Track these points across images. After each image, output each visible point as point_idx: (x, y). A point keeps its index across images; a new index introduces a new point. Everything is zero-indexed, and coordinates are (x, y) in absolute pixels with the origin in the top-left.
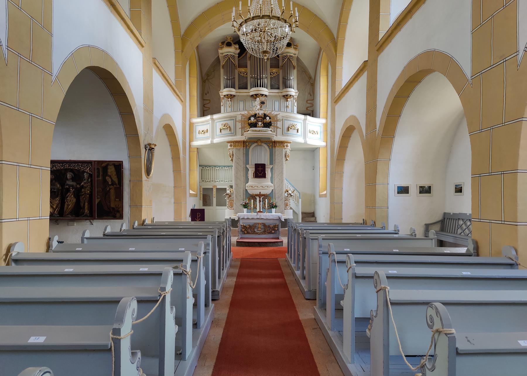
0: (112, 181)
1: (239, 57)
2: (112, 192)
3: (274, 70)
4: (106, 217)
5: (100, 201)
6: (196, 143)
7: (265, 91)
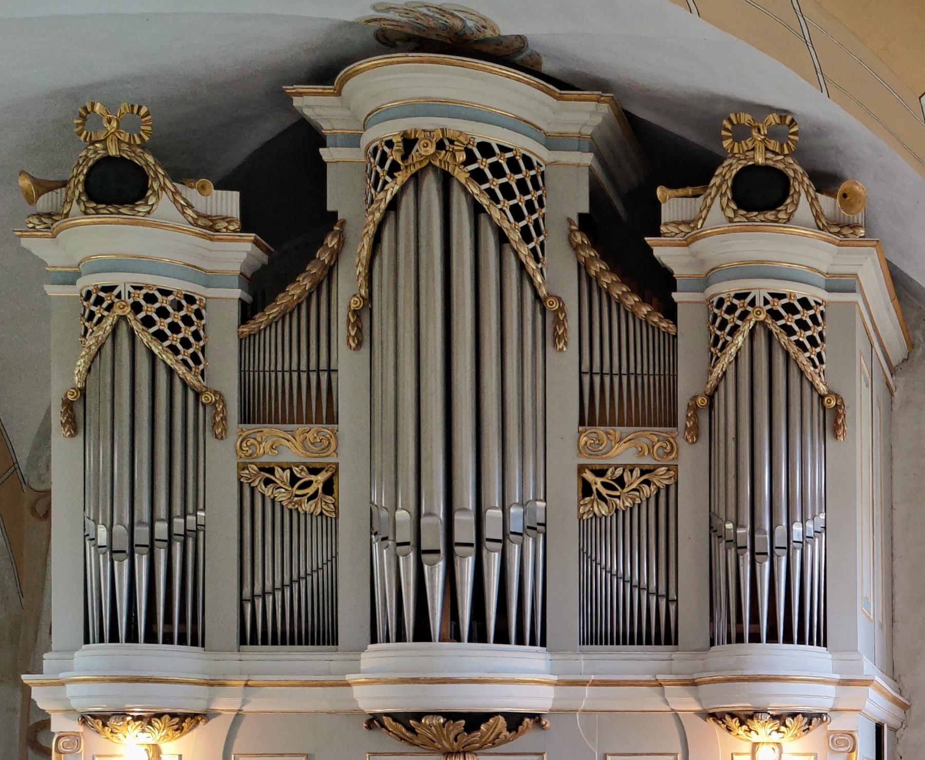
3: (624, 449)
7: (513, 678)
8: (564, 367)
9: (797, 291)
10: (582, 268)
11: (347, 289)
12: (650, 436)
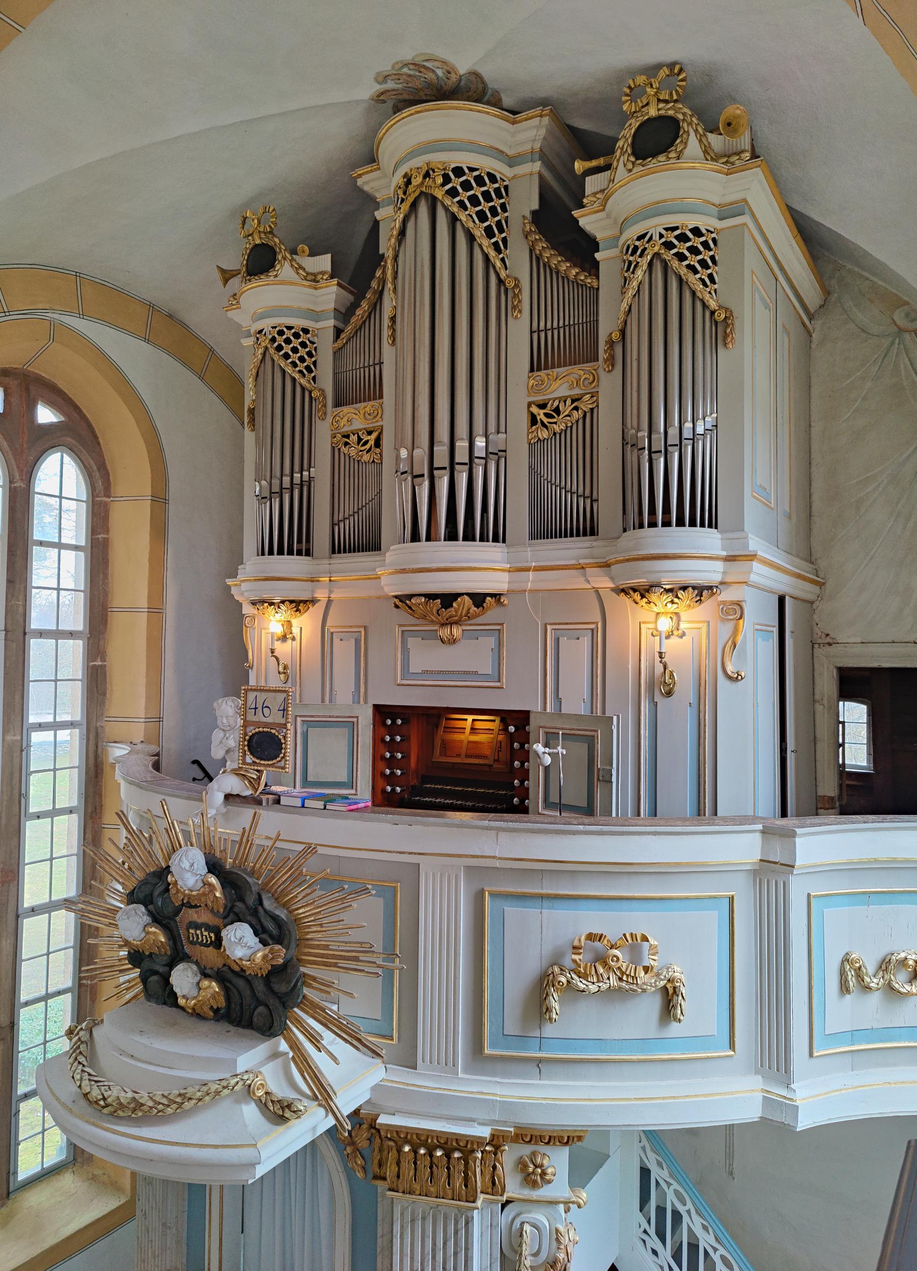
1: (338, 332)
3: (560, 385)
7: (480, 567)
12: (578, 371)
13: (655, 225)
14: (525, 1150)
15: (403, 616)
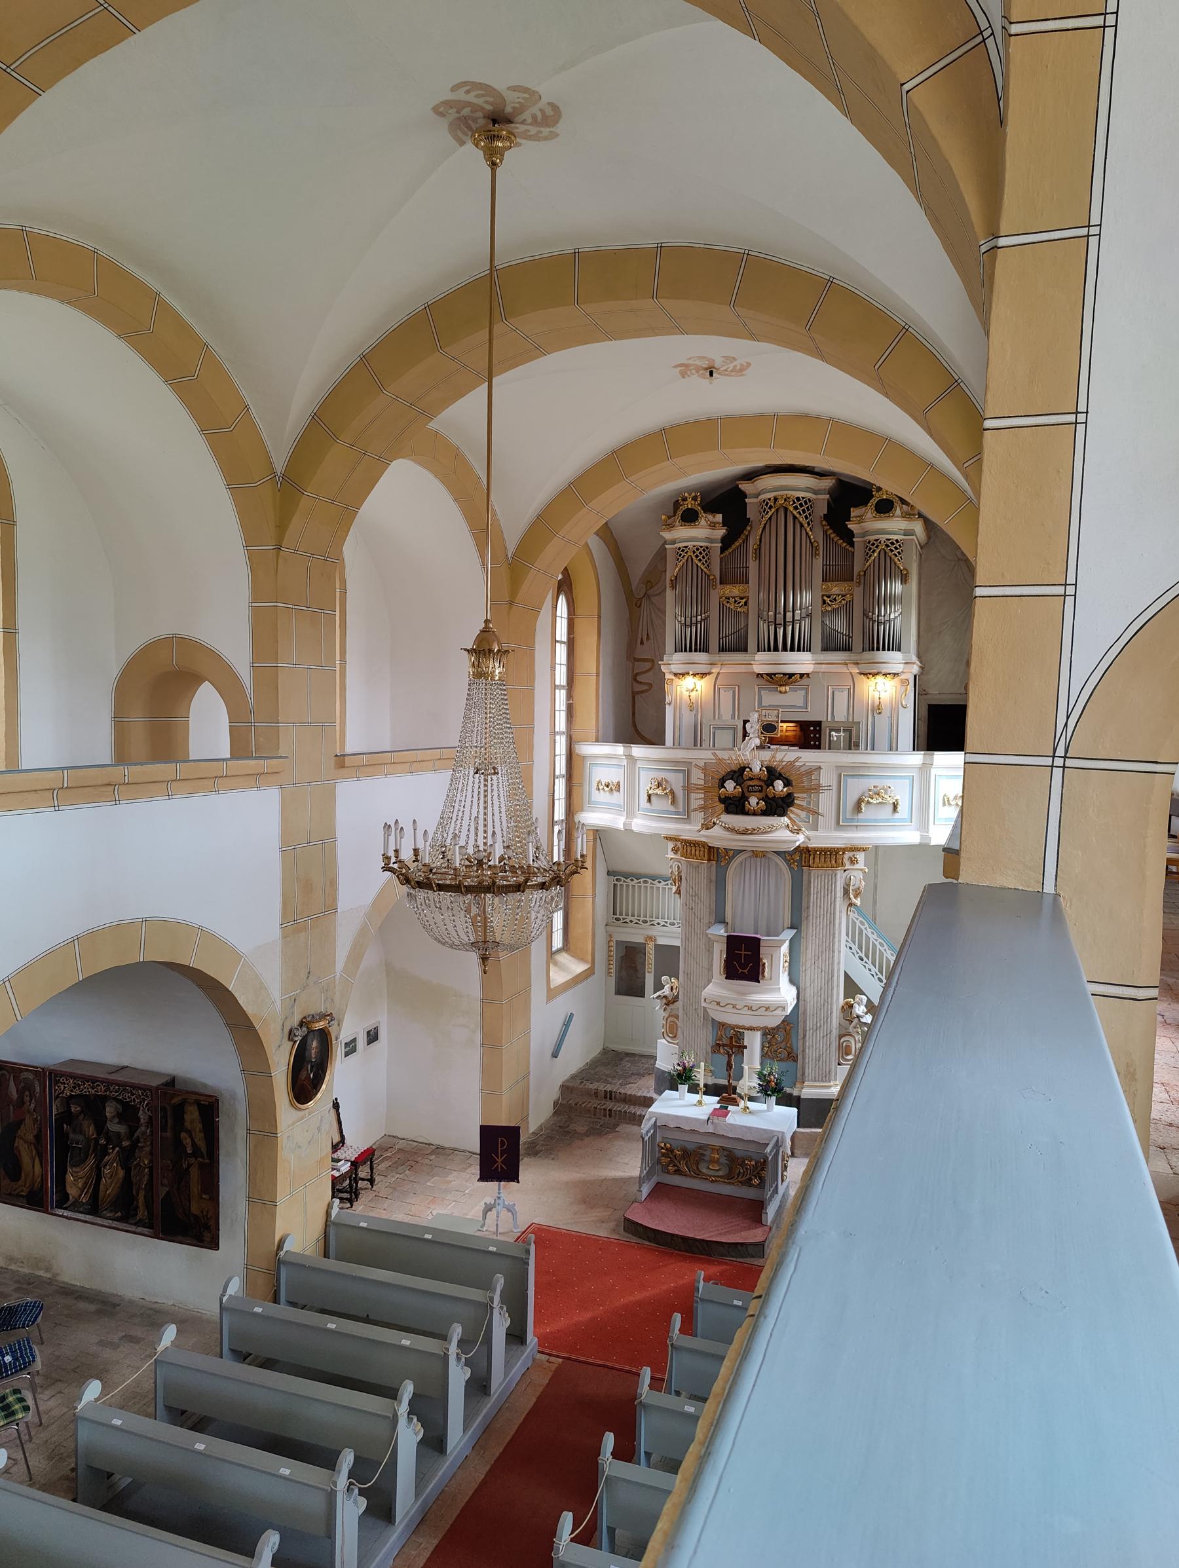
0: (194, 1144)
1: (723, 550)
2: (194, 1173)
3: (836, 589)
4: (180, 1238)
5: (168, 1193)
6: (591, 818)
7: (801, 662)
8: (818, 563)
9: (896, 537)
10: (825, 532)
11: (753, 543)
12: (845, 584)
13: (883, 538)
14: (851, 854)
15: (761, 681)
